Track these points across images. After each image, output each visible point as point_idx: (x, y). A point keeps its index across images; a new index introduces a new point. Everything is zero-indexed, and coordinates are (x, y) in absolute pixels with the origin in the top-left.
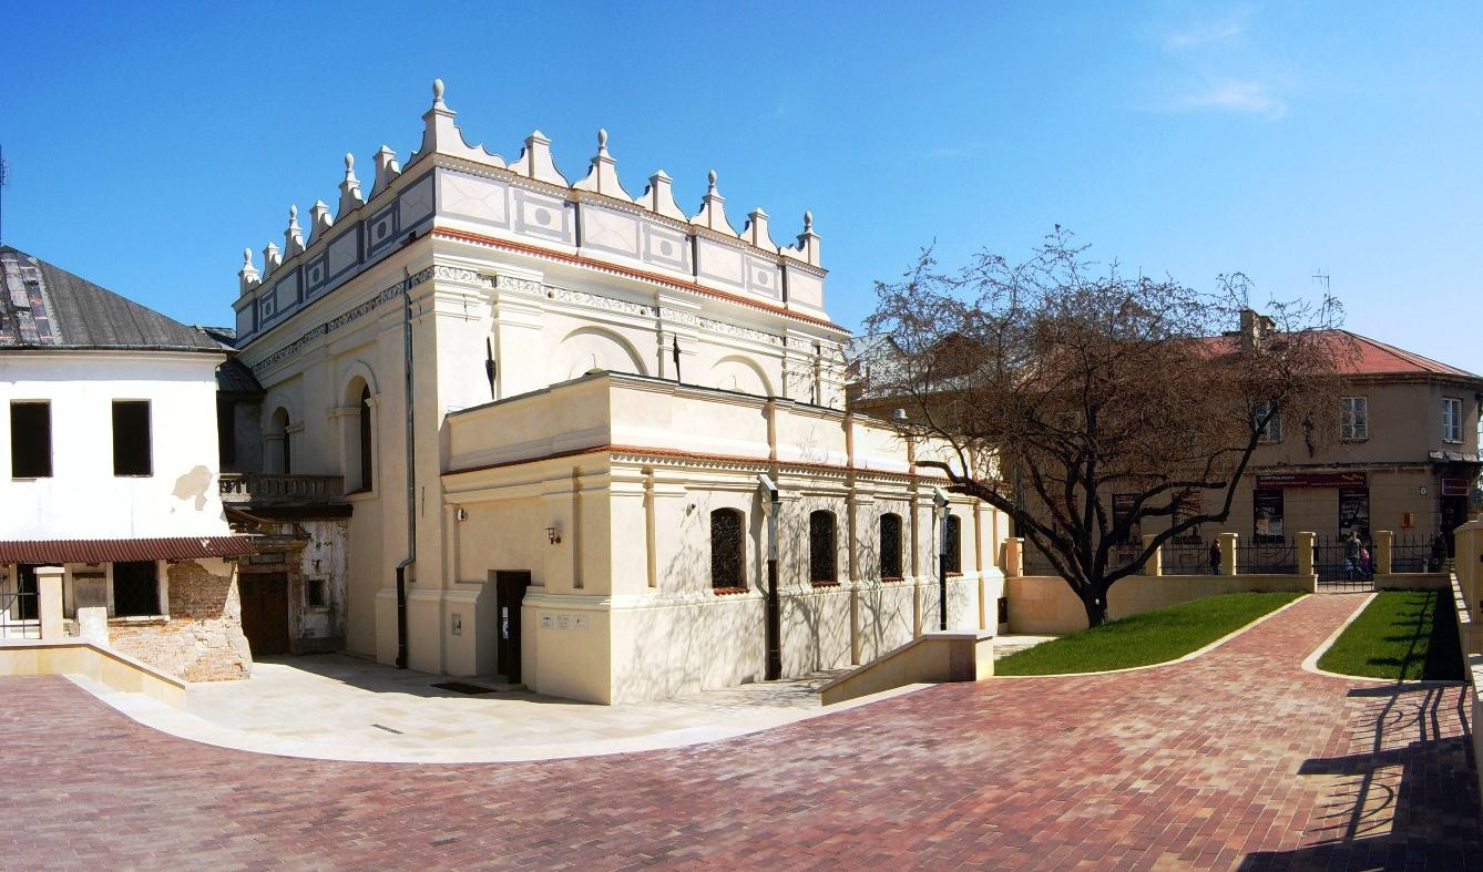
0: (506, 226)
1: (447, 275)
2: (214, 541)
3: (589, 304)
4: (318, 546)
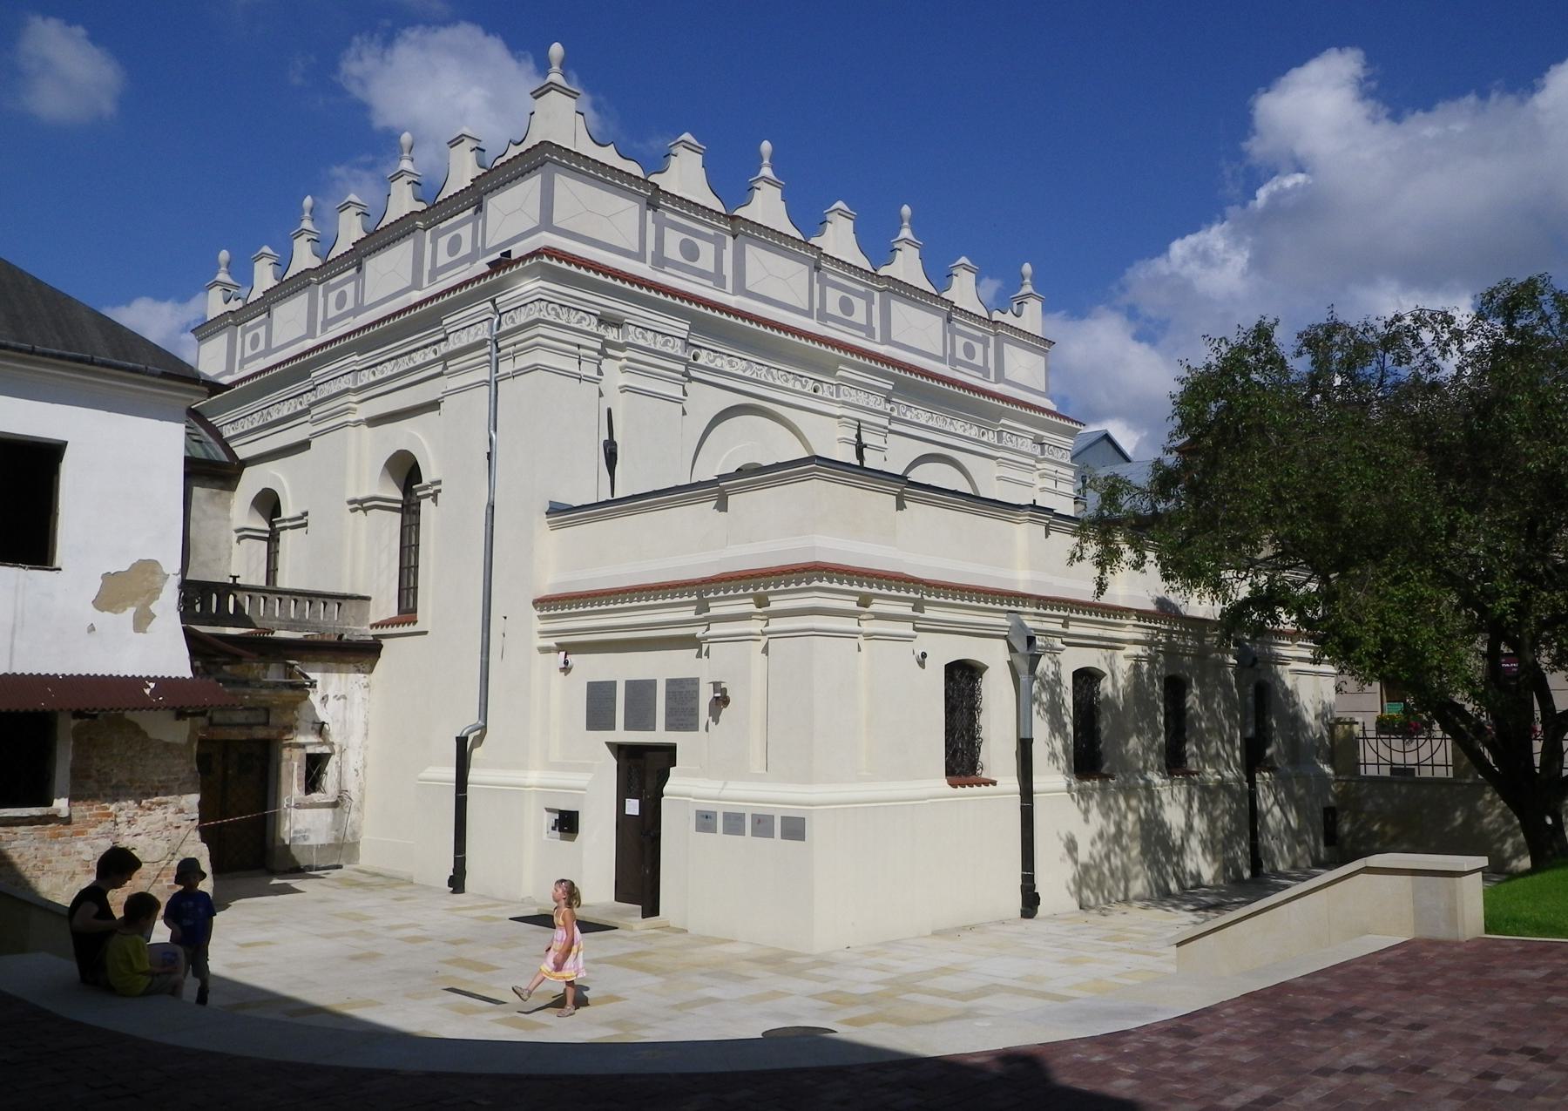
0: (640, 256)
1: (558, 315)
2: (165, 684)
3: (747, 374)
4: (324, 699)
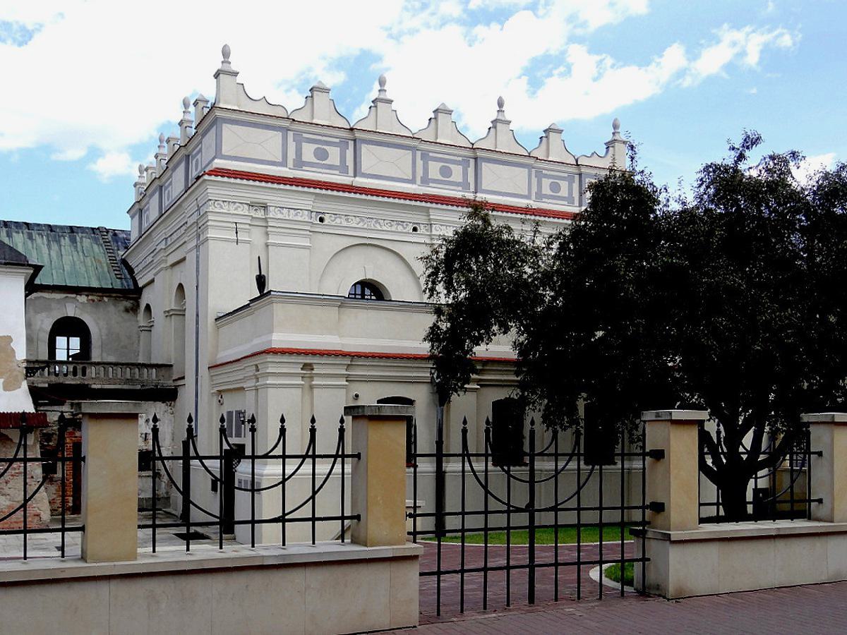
1: (221, 207)
